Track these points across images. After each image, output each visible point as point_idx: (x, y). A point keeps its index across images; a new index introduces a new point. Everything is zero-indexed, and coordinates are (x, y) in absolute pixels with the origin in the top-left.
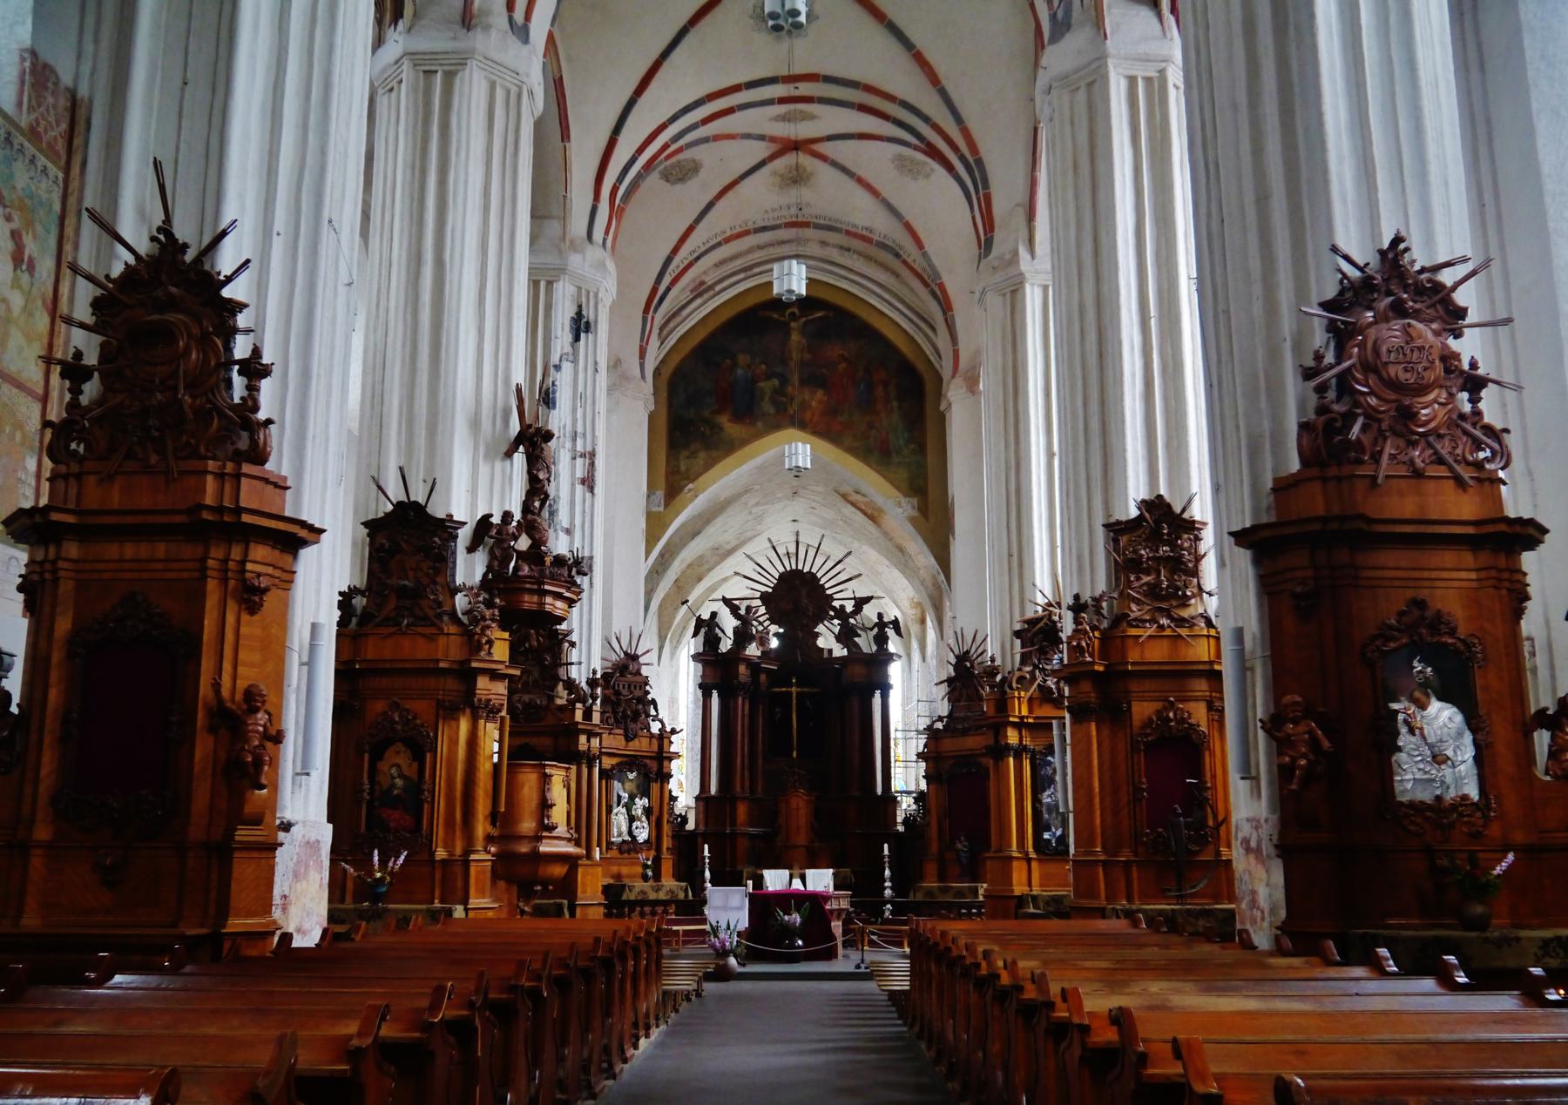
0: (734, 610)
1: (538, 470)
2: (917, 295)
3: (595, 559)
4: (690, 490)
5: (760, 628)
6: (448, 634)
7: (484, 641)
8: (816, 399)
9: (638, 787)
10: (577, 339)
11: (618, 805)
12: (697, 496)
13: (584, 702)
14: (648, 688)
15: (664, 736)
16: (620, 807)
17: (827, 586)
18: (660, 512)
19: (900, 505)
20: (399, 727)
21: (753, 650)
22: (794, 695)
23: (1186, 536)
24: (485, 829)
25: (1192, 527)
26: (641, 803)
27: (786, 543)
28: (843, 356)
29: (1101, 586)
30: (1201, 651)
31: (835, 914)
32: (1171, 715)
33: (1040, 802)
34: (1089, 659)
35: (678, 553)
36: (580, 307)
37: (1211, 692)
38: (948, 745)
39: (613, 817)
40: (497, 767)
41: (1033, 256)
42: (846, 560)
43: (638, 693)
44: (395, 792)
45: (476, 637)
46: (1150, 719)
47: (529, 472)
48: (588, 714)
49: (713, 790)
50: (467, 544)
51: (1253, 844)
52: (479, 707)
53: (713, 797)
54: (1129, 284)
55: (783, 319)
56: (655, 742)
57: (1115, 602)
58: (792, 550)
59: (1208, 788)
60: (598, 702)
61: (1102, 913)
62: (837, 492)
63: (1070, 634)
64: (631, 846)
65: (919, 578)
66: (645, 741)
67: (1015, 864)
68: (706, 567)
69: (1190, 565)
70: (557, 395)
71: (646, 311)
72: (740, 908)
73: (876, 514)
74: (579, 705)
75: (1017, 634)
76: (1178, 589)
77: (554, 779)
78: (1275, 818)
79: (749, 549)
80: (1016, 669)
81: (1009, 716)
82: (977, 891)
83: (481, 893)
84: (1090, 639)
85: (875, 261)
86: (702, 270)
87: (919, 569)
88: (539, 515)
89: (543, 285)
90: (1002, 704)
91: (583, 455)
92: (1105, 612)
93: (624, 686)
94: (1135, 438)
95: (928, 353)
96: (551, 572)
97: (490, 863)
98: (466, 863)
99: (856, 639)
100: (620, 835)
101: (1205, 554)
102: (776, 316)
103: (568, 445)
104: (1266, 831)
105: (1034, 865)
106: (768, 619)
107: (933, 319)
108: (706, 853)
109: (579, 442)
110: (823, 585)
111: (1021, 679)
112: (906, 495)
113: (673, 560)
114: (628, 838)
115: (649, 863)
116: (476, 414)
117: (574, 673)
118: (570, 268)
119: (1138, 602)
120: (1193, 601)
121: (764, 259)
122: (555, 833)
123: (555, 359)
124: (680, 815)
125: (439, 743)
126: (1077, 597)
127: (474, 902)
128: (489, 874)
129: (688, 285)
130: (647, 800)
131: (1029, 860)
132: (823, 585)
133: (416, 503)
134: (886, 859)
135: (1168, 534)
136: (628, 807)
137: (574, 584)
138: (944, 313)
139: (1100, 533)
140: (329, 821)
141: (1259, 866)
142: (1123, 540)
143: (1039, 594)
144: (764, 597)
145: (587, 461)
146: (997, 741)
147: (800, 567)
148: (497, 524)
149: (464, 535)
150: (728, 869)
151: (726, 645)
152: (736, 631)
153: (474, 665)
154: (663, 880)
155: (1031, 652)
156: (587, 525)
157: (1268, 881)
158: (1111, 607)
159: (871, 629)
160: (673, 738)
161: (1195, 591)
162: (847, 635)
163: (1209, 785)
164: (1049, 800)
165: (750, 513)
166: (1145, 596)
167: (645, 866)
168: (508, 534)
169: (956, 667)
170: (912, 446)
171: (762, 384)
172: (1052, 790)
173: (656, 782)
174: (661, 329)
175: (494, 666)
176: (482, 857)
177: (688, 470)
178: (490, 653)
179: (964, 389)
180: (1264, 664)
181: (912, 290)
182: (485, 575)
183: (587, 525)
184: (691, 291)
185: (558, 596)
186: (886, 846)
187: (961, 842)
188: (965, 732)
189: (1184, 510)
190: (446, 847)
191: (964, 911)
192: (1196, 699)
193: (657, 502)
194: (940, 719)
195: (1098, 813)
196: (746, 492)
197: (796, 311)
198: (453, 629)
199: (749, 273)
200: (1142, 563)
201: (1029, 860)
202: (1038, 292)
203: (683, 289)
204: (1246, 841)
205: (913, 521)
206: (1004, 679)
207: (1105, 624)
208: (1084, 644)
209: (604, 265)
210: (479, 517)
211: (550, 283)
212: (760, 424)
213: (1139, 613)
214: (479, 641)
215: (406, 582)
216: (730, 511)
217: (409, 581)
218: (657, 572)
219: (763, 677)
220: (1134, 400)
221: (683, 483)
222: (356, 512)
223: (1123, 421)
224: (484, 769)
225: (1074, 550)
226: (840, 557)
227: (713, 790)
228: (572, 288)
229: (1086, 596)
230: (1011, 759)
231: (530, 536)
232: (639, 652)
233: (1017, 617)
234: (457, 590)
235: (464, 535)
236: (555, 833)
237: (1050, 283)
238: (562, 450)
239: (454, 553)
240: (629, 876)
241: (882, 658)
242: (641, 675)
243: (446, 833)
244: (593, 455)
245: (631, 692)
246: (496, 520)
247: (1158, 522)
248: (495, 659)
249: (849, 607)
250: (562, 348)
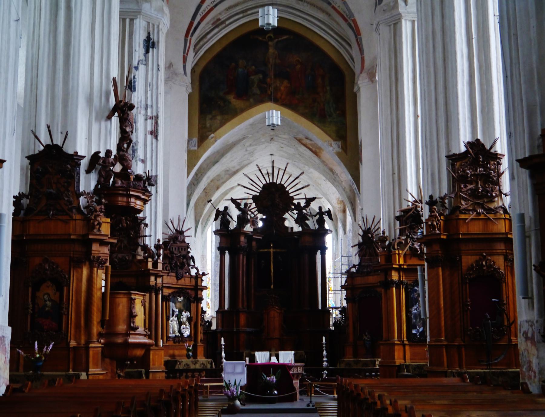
0: (238, 205)
1: (126, 126)
2: (340, 26)
3: (158, 177)
4: (212, 138)
5: (252, 216)
6: (76, 220)
7: (96, 223)
8: (284, 86)
9: (184, 306)
10: (147, 52)
11: (173, 316)
12: (216, 141)
13: (153, 257)
14: (189, 250)
15: (199, 277)
16: (174, 317)
18: (195, 150)
19: (331, 146)
20: (48, 272)
21: (248, 228)
22: (272, 253)
23: (492, 162)
24: (97, 330)
25: (496, 158)
26: (185, 315)
27: (267, 167)
28: (298, 61)
29: (445, 191)
30: (501, 227)
31: (295, 376)
32: (484, 263)
33: (410, 312)
34: (438, 232)
35: (206, 173)
36: (149, 33)
37: (506, 250)
38: (359, 281)
39: (170, 322)
40: (104, 295)
41: (406, 4)
42: (301, 177)
43: (183, 253)
44: (47, 309)
45: (92, 221)
46: (472, 265)
47: (121, 127)
48: (155, 265)
49: (226, 307)
50: (86, 168)
51: (530, 335)
52: (94, 261)
53: (226, 311)
54: (460, 19)
55: (264, 40)
56: (193, 281)
57: (453, 199)
58: (270, 171)
59: (505, 304)
60: (161, 257)
61: (445, 374)
62: (296, 138)
63: (427, 217)
64: (180, 339)
65: (342, 187)
66: (188, 280)
67: (396, 347)
68: (221, 181)
69: (495, 179)
70: (137, 83)
71: (187, 35)
72: (242, 373)
73: (318, 151)
74: (150, 260)
75: (397, 218)
76: (488, 192)
77: (137, 301)
78: (541, 320)
79: (246, 171)
80: (397, 238)
81: (393, 264)
82: (375, 363)
83: (96, 366)
84: (438, 220)
85: (317, 7)
86: (218, 12)
87: (342, 182)
88: (127, 152)
89: (128, 21)
90: (389, 257)
91: (151, 118)
92: (447, 205)
93: (175, 249)
94: (464, 107)
95: (347, 59)
96: (133, 184)
97: (100, 349)
98: (87, 349)
99: (307, 222)
100: (174, 332)
101: (503, 173)
102: (260, 38)
103: (143, 112)
104: (536, 327)
105: (407, 348)
106: (257, 210)
107: (350, 40)
108: (223, 343)
109: (149, 110)
110: (288, 191)
111: (400, 244)
112: (335, 140)
113: (203, 177)
114: (178, 334)
115: (191, 348)
116: (90, 95)
117: (147, 241)
118: (143, 11)
119: (465, 199)
120: (496, 199)
121: (254, 6)
122: (137, 332)
123: (135, 63)
124: (208, 321)
125: (71, 281)
126: (431, 197)
127: (92, 370)
128: (100, 355)
129: (211, 20)
130: (189, 313)
131: (404, 345)
132: (288, 191)
133: (57, 145)
134: (324, 345)
135: (482, 161)
136: (179, 317)
137: (147, 191)
138: (356, 37)
139: (444, 161)
140: (9, 325)
141: (533, 347)
142: (457, 165)
143: (410, 196)
144: (255, 198)
145: (154, 121)
146: (386, 278)
147: (275, 181)
148: (103, 157)
149: (84, 163)
150: (235, 351)
151: (233, 225)
152: (239, 217)
153: (91, 237)
154: (198, 358)
155: (405, 228)
156: (154, 157)
157: (538, 355)
158: (450, 202)
159: (315, 216)
160: (204, 278)
161: (497, 193)
162: (301, 220)
163: (505, 302)
164: (416, 311)
165: (246, 150)
166: (469, 196)
167: (188, 350)
168: (109, 163)
169: (363, 237)
170: (338, 112)
171: (252, 77)
172: (417, 306)
173: (194, 303)
174: (195, 46)
175: (102, 238)
176: (96, 345)
177: (211, 126)
178: (99, 231)
179: (367, 80)
180: (536, 235)
181: (338, 23)
182: (96, 186)
183: (154, 157)
184: (212, 25)
185: (138, 198)
186: (324, 338)
187: (366, 335)
188: (368, 274)
189: (491, 148)
190: (75, 339)
191: (367, 374)
192: (498, 254)
193: (193, 144)
194: (354, 266)
195: (443, 318)
196: (244, 138)
197: (272, 35)
198: (78, 217)
199: (245, 14)
200: (468, 177)
201: (404, 345)
202: (409, 25)
203: (208, 23)
204: (525, 333)
205: (338, 154)
206: (390, 244)
207: (447, 212)
208: (435, 224)
209: (163, 9)
210: (93, 153)
211: (132, 20)
212: (251, 100)
213: (466, 206)
214: (93, 224)
215: (52, 190)
216: (235, 149)
217: (53, 190)
218: (194, 184)
219: (254, 243)
220: (463, 85)
221: (208, 133)
222: (23, 150)
223: (457, 97)
224: (97, 295)
225: (429, 170)
226: (298, 175)
227: (226, 307)
228: (144, 22)
229: (436, 196)
230: (394, 289)
231: (122, 164)
232: (184, 230)
233: (397, 208)
234: (81, 195)
235: (84, 163)
236: (137, 332)
237: (416, 19)
238: (139, 115)
239: (79, 174)
240: (180, 356)
241: (322, 232)
242: (185, 242)
243: (76, 332)
244: (157, 117)
245: (180, 252)
246: (102, 155)
247: (477, 155)
248: (103, 233)
249: (303, 204)
250: (139, 57)
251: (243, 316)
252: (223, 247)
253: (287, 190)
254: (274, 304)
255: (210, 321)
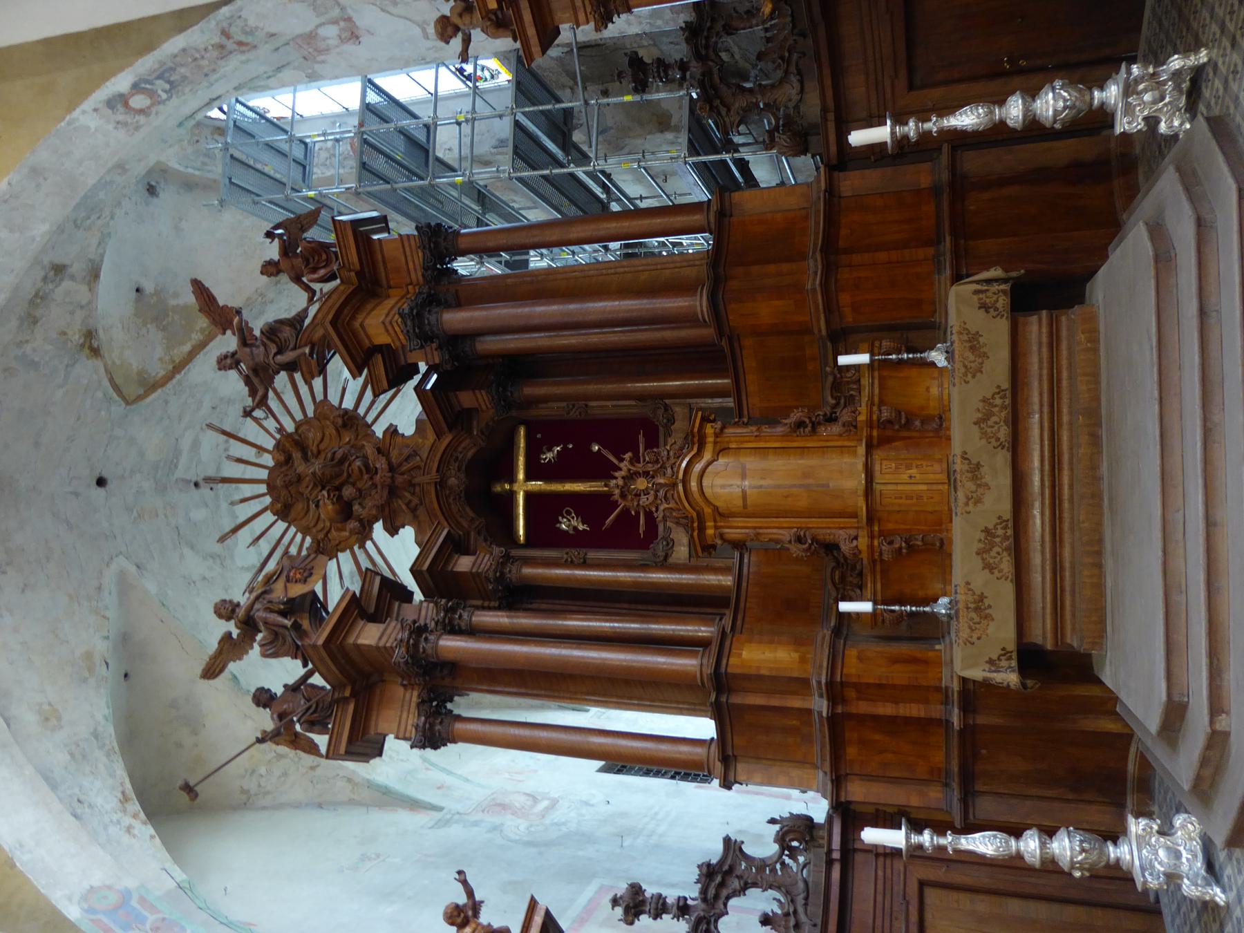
0: (230, 649)
17: (299, 416)
106: (362, 546)
124: (782, 839)
132: (298, 425)
147: (264, 474)
152: (274, 649)
219: (464, 564)
251: (745, 654)
252: (417, 727)
253: (290, 427)
254: (662, 481)
255: (777, 827)
